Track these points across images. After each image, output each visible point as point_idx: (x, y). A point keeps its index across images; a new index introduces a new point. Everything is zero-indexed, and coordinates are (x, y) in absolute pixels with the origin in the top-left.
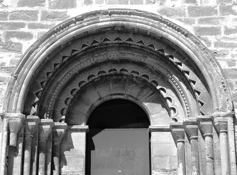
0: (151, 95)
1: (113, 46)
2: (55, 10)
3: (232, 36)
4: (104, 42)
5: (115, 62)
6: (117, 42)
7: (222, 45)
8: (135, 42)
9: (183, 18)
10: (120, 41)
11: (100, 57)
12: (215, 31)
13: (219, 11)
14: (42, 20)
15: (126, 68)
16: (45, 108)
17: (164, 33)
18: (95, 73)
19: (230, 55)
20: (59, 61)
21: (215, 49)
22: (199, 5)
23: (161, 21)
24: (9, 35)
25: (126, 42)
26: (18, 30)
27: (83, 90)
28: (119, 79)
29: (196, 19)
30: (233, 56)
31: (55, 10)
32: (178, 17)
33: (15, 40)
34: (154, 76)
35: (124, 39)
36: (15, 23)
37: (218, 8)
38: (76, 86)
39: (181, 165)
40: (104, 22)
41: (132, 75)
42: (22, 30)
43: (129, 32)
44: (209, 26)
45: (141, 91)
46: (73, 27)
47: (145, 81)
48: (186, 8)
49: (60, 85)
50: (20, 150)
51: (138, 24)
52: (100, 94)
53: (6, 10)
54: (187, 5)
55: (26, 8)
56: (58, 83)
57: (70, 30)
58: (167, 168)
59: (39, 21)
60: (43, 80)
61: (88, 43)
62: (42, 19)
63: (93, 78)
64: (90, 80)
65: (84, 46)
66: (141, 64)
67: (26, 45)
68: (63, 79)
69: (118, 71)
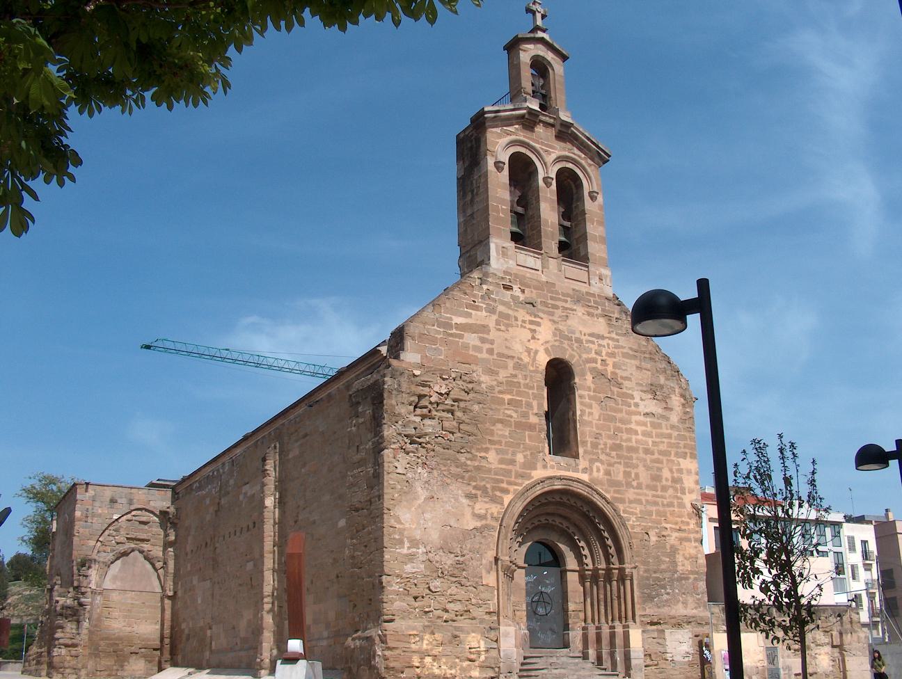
2: (524, 471)
3: (632, 505)
5: (548, 514)
9: (604, 488)
12: (622, 501)
14: (515, 478)
17: (595, 500)
23: (593, 489)
24: (494, 489)
26: (499, 485)
29: (612, 489)
30: (633, 521)
31: (524, 471)
33: (498, 493)
36: (498, 479)
37: (624, 482)
40: (558, 486)
44: (620, 496)
46: (539, 487)
51: (579, 490)
53: (490, 466)
54: (606, 477)
55: (503, 466)
57: (536, 490)
58: (578, 601)
59: (513, 479)
66: (565, 518)
67: (507, 499)
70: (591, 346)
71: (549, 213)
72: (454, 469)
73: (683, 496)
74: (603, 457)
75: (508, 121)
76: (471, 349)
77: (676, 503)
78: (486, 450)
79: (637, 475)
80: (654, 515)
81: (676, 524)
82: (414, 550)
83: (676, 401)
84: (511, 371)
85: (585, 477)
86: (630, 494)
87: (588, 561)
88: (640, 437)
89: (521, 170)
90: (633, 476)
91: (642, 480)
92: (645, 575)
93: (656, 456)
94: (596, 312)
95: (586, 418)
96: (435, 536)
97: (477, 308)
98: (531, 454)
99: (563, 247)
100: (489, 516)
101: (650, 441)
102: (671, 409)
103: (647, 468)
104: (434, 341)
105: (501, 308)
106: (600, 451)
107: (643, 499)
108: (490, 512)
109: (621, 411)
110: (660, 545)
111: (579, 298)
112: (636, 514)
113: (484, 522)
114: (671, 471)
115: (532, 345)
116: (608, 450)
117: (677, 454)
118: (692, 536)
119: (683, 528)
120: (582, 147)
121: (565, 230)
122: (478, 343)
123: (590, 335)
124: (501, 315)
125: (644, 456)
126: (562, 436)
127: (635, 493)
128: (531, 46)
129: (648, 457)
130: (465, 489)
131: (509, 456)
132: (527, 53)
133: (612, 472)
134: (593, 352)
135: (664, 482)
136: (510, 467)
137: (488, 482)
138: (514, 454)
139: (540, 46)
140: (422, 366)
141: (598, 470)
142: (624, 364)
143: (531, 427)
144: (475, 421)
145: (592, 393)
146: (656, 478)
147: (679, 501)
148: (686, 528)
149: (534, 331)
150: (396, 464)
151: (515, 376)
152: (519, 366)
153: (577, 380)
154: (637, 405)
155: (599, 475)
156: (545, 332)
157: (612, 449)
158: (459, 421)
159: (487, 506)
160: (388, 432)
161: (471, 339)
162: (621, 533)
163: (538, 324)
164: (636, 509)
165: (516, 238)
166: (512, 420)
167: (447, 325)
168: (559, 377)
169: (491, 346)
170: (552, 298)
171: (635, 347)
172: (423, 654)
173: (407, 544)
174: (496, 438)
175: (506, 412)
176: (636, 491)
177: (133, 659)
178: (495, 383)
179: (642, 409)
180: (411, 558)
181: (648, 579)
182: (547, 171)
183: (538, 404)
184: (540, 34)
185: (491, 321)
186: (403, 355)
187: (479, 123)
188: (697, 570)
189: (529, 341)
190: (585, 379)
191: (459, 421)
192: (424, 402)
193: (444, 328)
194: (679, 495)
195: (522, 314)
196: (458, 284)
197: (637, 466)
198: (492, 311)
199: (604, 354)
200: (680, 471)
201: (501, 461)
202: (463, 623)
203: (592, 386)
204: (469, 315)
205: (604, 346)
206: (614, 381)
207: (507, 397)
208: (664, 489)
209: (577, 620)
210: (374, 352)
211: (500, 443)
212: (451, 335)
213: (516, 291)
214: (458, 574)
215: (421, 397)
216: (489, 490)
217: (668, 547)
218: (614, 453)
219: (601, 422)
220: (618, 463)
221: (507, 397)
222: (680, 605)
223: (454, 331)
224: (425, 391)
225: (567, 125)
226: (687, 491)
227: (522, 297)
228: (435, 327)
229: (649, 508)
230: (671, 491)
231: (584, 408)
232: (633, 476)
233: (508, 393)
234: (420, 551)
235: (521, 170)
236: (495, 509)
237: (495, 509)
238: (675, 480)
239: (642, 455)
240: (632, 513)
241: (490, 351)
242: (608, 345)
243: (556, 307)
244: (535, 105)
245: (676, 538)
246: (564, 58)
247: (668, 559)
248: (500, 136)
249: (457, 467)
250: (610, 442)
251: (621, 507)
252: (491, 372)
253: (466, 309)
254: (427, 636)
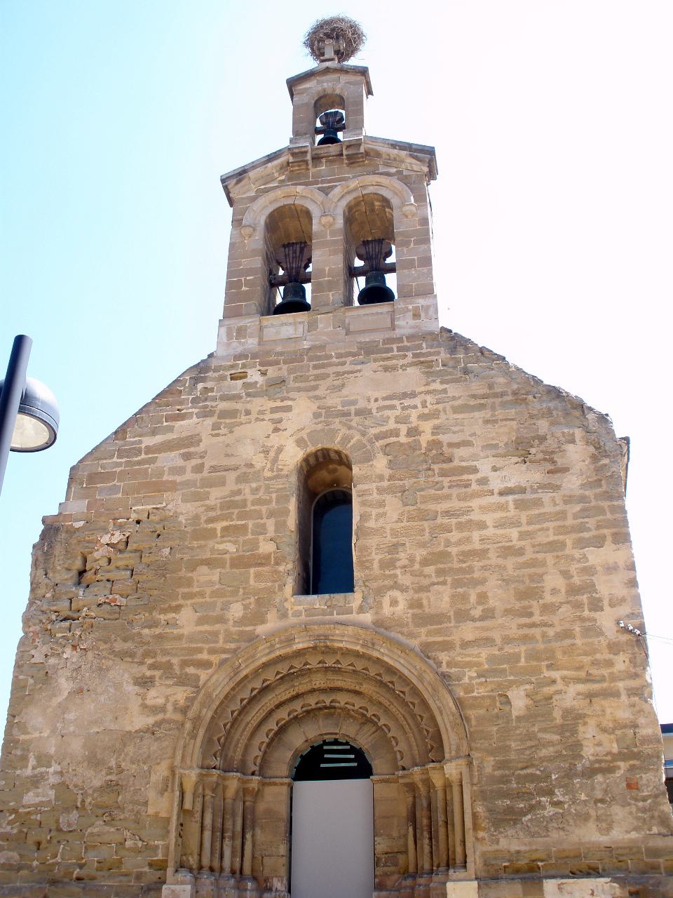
0: (373, 733)
1: (318, 670)
3: (469, 651)
4: (305, 667)
6: (321, 665)
7: (456, 665)
8: (344, 664)
9: (405, 630)
10: (325, 665)
11: (302, 686)
12: (447, 646)
13: (452, 617)
15: (338, 699)
16: (232, 756)
18: (297, 706)
19: (467, 678)
20: (246, 695)
21: (447, 670)
22: (427, 610)
24: (184, 664)
25: (333, 665)
26: (195, 657)
27: (282, 730)
28: (329, 711)
29: (423, 630)
30: (471, 678)
31: (241, 629)
32: (399, 629)
33: (191, 670)
34: (374, 708)
35: (330, 662)
37: (452, 614)
38: (272, 725)
39: (411, 829)
41: (347, 707)
42: (199, 656)
43: (337, 653)
44: (440, 639)
45: (361, 728)
47: (363, 715)
48: (409, 615)
49: (250, 725)
50: (198, 815)
52: (307, 735)
54: (410, 611)
55: (206, 628)
56: (248, 723)
59: (221, 644)
60: (226, 721)
61: (283, 668)
62: (226, 642)
63: (295, 714)
64: (291, 716)
65: (278, 673)
68: (255, 715)
69: (328, 704)
70: (387, 413)
72: (119, 646)
73: (597, 615)
74: (405, 580)
76: (166, 473)
77: (578, 629)
78: (177, 609)
79: (482, 598)
80: (523, 660)
81: (579, 668)
82: (43, 769)
83: (577, 454)
84: (231, 485)
86: (468, 631)
88: (490, 531)
90: (473, 598)
91: (492, 603)
92: (498, 773)
93: (529, 555)
94: (401, 362)
95: (371, 524)
98: (258, 601)
100: (170, 707)
101: (514, 533)
102: (565, 470)
105: (223, 405)
106: (398, 572)
107: (497, 636)
108: (172, 700)
109: (448, 497)
112: (479, 664)
113: (160, 717)
114: (566, 574)
115: (275, 440)
116: (417, 566)
117: (581, 544)
118: (621, 685)
119: (594, 671)
122: (180, 462)
123: (385, 399)
124: (224, 414)
125: (500, 561)
127: (477, 628)
129: (510, 563)
130: (134, 671)
131: (217, 612)
133: (425, 602)
134: (392, 421)
135: (548, 598)
136: (217, 626)
137: (176, 655)
138: (225, 607)
141: (394, 603)
142: (457, 425)
143: (263, 561)
145: (386, 484)
146: (531, 593)
147: (587, 624)
148: (605, 672)
149: (280, 421)
150: (33, 652)
151: (239, 492)
152: (247, 474)
154: (483, 481)
157: (425, 562)
159: (169, 691)
161: (170, 459)
163: (289, 409)
164: (478, 655)
166: (227, 556)
169: (199, 461)
170: (315, 367)
171: (481, 392)
173: (32, 761)
174: (196, 589)
175: (217, 546)
176: (478, 624)
178: (202, 509)
179: (496, 484)
180: (36, 781)
181: (505, 780)
183: (276, 524)
188: (635, 750)
189: (268, 437)
190: (372, 466)
193: (127, 457)
194: (586, 613)
197: (483, 581)
199: (414, 418)
200: (589, 571)
201: (200, 621)
203: (387, 472)
204: (171, 429)
205: (415, 407)
207: (219, 526)
208: (548, 609)
209: (392, 869)
211: (202, 594)
212: (139, 463)
213: (254, 376)
216: (176, 668)
217: (557, 714)
218: (430, 570)
219: (405, 524)
220: (438, 583)
221: (219, 526)
222: (592, 825)
223: (143, 456)
226: (606, 603)
228: (115, 459)
229: (509, 649)
231: (368, 509)
232: (473, 598)
233: (223, 520)
234: (51, 770)
238: (573, 590)
240: (469, 665)
242: (424, 405)
243: (324, 377)
245: (578, 694)
247: (556, 738)
249: (125, 640)
250: (420, 553)
251: (444, 657)
253: (165, 424)
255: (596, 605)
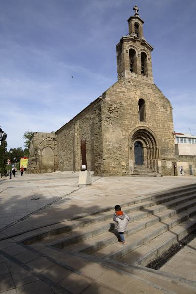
67: (130, 131)
71: (139, 63)
75: (129, 40)
83: (168, 109)
85: (148, 126)
86: (158, 130)
87: (148, 145)
89: (132, 52)
96: (114, 140)
97: (122, 87)
99: (142, 72)
103: (162, 124)
104: (113, 95)
110: (165, 142)
111: (146, 84)
115: (136, 96)
120: (147, 47)
121: (142, 68)
122: (123, 95)
124: (128, 89)
126: (142, 117)
128: (134, 19)
132: (134, 21)
139: (137, 19)
140: (110, 101)
143: (136, 115)
144: (122, 113)
146: (164, 127)
153: (146, 104)
155: (151, 126)
156: (138, 93)
158: (118, 113)
160: (103, 116)
161: (121, 94)
162: (156, 139)
165: (131, 70)
167: (116, 91)
168: (141, 103)
172: (113, 167)
177: (49, 169)
179: (161, 111)
180: (109, 145)
182: (138, 53)
184: (137, 16)
185: (126, 90)
186: (106, 98)
187: (122, 41)
191: (118, 113)
192: (111, 109)
195: (133, 88)
196: (117, 82)
198: (126, 88)
201: (129, 123)
202: (121, 160)
204: (120, 89)
206: (154, 104)
208: (166, 129)
210: (99, 98)
213: (131, 83)
214: (119, 149)
215: (110, 108)
224: (111, 107)
225: (143, 41)
227: (133, 84)
230: (167, 130)
235: (132, 52)
236: (128, 134)
237: (128, 134)
239: (160, 121)
241: (126, 97)
244: (135, 35)
246: (143, 22)
248: (127, 44)
252: (126, 102)
254: (113, 163)
255: (170, 129)
